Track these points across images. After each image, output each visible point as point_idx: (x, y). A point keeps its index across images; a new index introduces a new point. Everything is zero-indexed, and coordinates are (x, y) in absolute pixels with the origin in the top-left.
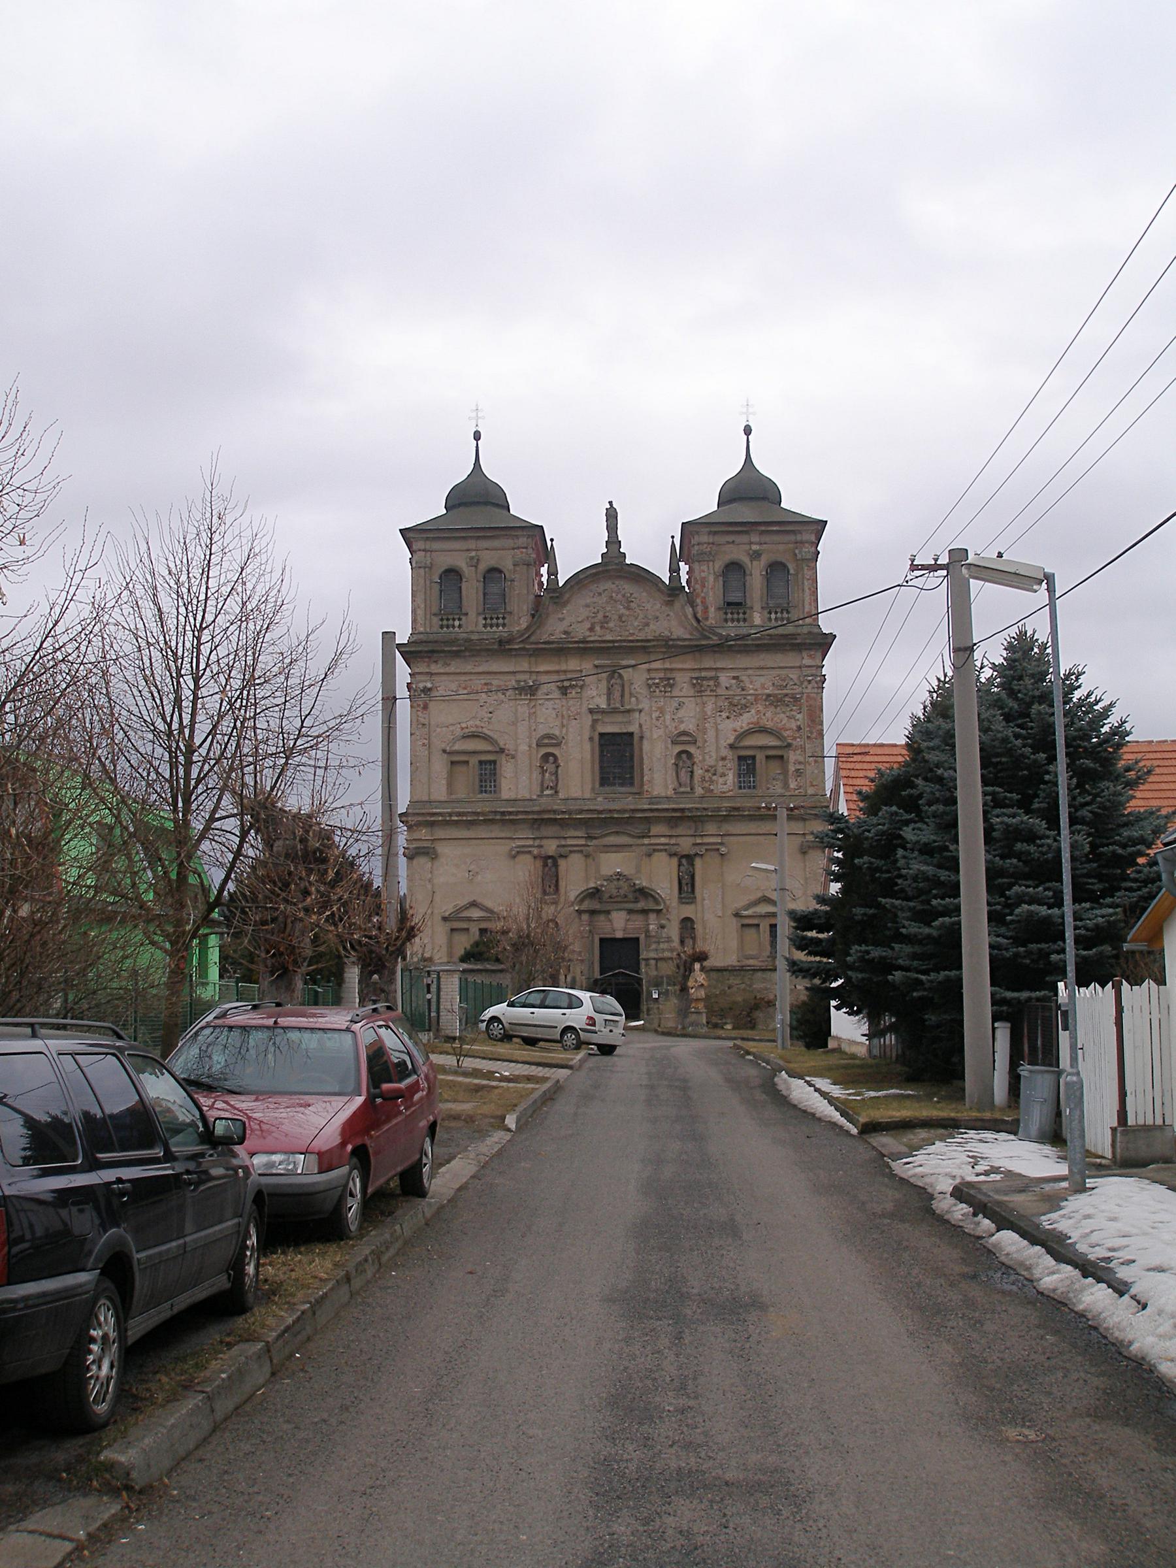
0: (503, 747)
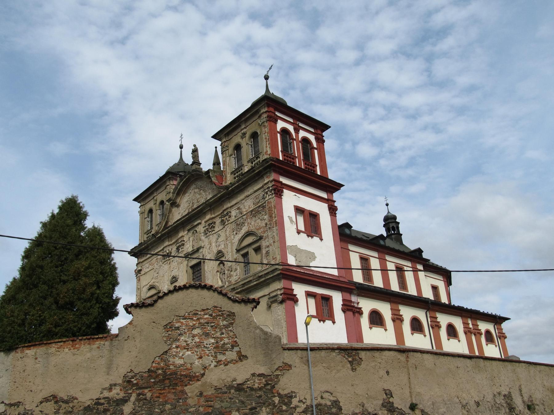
0: (160, 289)
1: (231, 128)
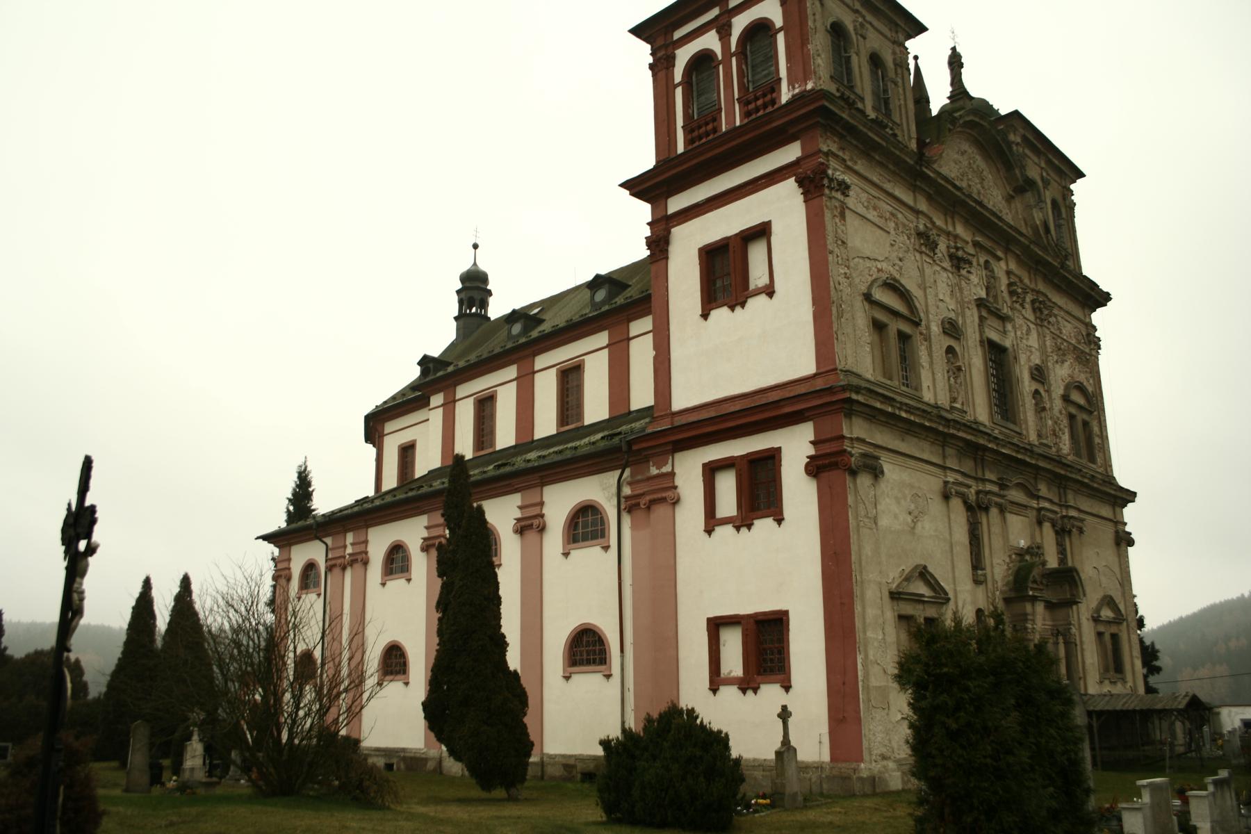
1: (1035, 142)
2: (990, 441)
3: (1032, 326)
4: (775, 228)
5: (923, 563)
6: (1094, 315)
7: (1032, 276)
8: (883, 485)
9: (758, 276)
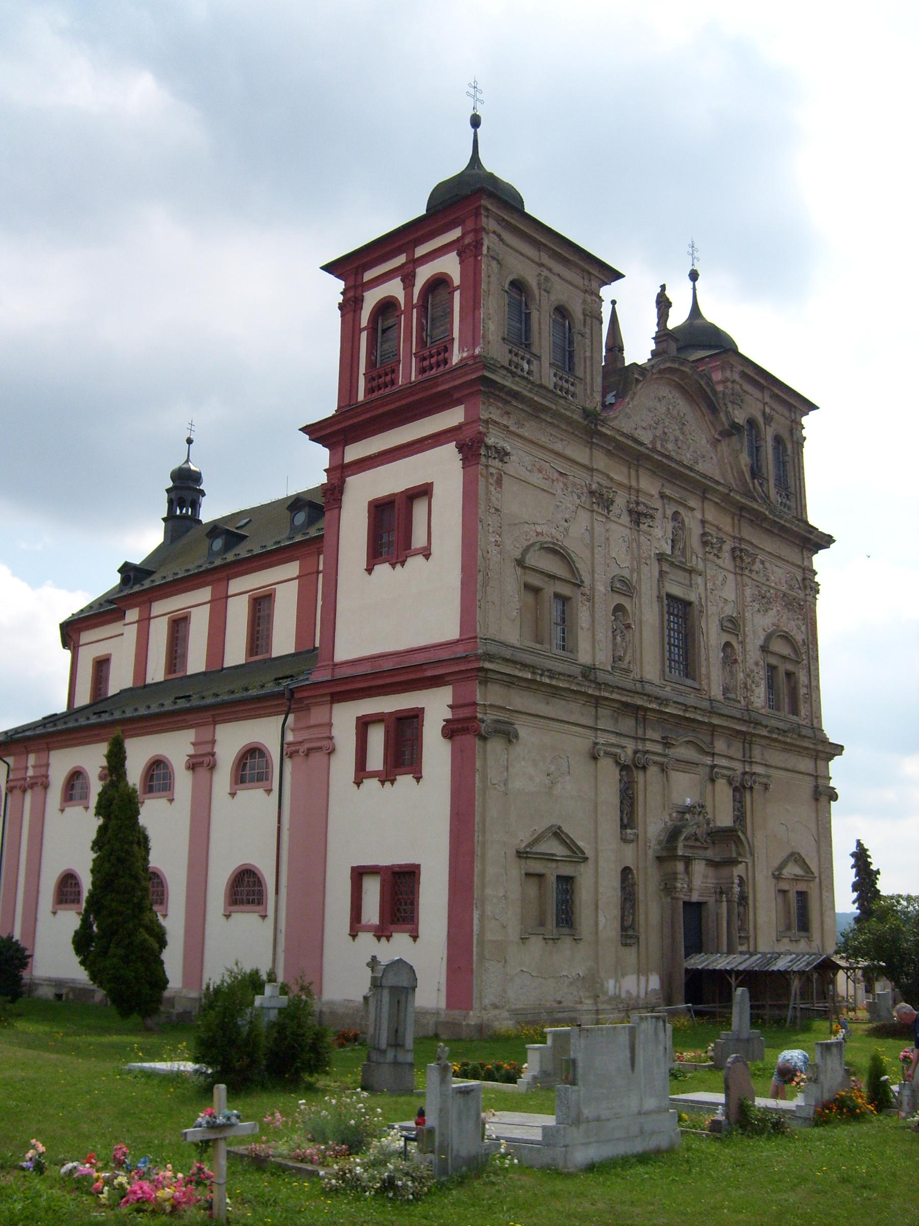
1: (756, 377)
2: (650, 702)
3: (731, 577)
4: (436, 491)
5: (559, 823)
6: (815, 558)
7: (736, 521)
8: (518, 750)
9: (419, 539)
